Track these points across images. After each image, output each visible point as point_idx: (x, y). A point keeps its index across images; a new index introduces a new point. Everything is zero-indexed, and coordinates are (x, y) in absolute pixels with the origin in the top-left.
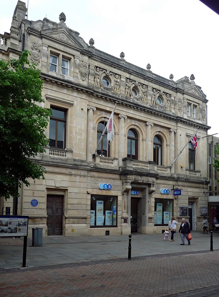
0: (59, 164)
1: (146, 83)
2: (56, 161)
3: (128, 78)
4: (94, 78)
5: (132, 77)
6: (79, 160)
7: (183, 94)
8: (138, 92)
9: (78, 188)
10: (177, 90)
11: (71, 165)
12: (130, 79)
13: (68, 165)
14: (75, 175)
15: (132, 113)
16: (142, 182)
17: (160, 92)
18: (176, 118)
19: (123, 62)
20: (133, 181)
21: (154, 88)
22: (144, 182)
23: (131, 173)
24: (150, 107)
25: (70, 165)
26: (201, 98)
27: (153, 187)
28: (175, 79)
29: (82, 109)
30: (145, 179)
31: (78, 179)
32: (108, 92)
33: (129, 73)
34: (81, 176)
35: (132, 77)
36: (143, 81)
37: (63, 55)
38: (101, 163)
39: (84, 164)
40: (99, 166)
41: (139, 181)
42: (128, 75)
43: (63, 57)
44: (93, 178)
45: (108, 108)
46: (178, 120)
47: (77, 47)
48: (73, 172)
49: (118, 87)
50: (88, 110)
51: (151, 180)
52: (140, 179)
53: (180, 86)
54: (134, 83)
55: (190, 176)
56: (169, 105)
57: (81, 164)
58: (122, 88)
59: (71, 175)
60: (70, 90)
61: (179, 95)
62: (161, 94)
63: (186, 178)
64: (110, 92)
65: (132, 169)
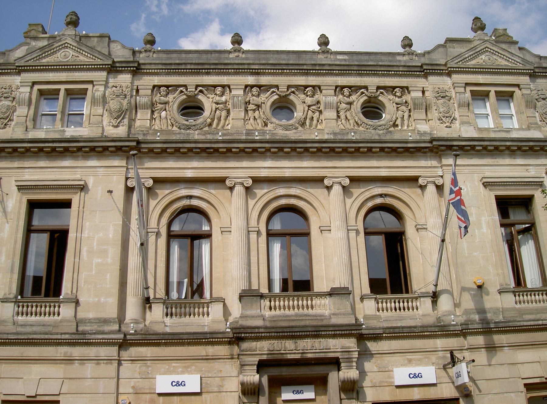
0: (35, 336)
1: (313, 80)
2: (28, 329)
3: (252, 86)
4: (153, 112)
5: (264, 80)
6: (95, 319)
7: (449, 74)
8: (295, 108)
9: (88, 395)
10: (425, 70)
11: (67, 336)
12: (259, 87)
13: (59, 337)
14: (83, 360)
15: (266, 167)
16: (298, 356)
17: (367, 90)
18: (429, 145)
19: (236, 54)
20: (265, 357)
21: (343, 87)
22: (310, 356)
23: (256, 334)
24: (332, 137)
25: (64, 337)
26: (520, 66)
27: (350, 367)
28: (418, 48)
29: (110, 192)
30: (311, 347)
31: (89, 369)
32: (189, 134)
33: (252, 74)
34: (98, 360)
35: (264, 80)
36: (301, 80)
37: (66, 90)
38: (168, 320)
39: (107, 328)
40: (159, 329)
41: (290, 357)
42: (251, 80)
43: (69, 92)
44: (138, 365)
45: (190, 171)
46: (438, 148)
47: (99, 62)
48: (77, 352)
49: (224, 113)
50: (129, 190)
51: (334, 346)
52: (291, 349)
53: (440, 58)
54: (273, 92)
55: (519, 310)
56: (406, 115)
57: (101, 329)
58: (237, 113)
59: (69, 361)
60: (78, 156)
61: (434, 82)
62: (369, 95)
63: (503, 317)
64: (197, 132)
65: (259, 323)
